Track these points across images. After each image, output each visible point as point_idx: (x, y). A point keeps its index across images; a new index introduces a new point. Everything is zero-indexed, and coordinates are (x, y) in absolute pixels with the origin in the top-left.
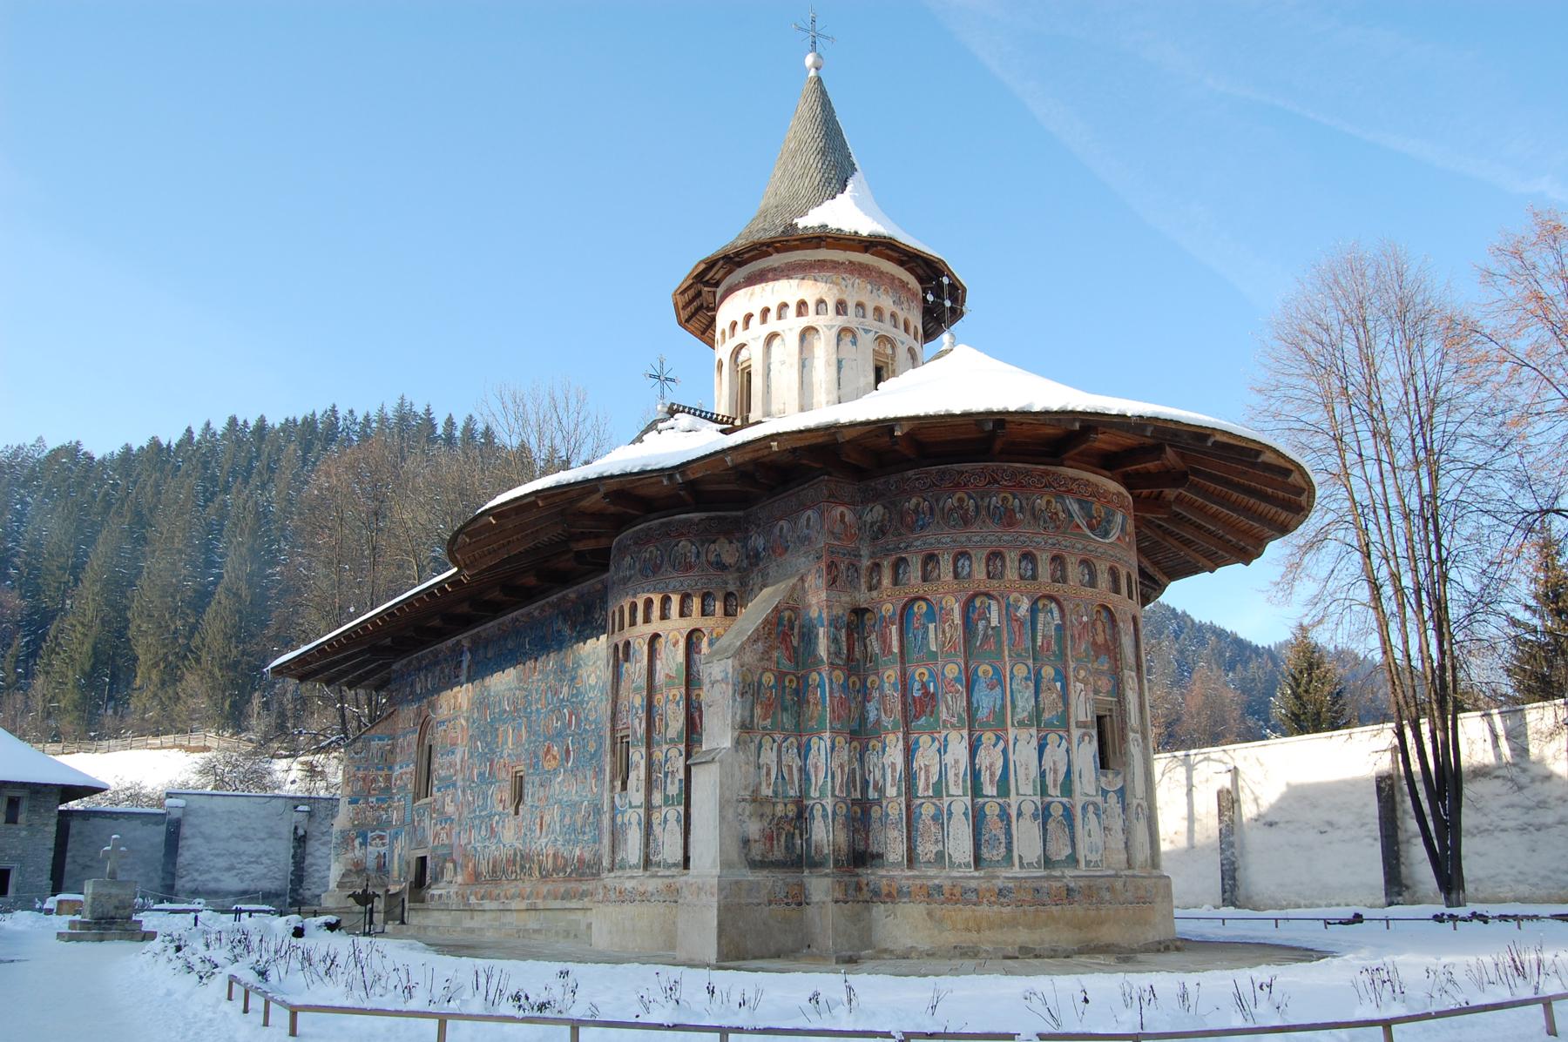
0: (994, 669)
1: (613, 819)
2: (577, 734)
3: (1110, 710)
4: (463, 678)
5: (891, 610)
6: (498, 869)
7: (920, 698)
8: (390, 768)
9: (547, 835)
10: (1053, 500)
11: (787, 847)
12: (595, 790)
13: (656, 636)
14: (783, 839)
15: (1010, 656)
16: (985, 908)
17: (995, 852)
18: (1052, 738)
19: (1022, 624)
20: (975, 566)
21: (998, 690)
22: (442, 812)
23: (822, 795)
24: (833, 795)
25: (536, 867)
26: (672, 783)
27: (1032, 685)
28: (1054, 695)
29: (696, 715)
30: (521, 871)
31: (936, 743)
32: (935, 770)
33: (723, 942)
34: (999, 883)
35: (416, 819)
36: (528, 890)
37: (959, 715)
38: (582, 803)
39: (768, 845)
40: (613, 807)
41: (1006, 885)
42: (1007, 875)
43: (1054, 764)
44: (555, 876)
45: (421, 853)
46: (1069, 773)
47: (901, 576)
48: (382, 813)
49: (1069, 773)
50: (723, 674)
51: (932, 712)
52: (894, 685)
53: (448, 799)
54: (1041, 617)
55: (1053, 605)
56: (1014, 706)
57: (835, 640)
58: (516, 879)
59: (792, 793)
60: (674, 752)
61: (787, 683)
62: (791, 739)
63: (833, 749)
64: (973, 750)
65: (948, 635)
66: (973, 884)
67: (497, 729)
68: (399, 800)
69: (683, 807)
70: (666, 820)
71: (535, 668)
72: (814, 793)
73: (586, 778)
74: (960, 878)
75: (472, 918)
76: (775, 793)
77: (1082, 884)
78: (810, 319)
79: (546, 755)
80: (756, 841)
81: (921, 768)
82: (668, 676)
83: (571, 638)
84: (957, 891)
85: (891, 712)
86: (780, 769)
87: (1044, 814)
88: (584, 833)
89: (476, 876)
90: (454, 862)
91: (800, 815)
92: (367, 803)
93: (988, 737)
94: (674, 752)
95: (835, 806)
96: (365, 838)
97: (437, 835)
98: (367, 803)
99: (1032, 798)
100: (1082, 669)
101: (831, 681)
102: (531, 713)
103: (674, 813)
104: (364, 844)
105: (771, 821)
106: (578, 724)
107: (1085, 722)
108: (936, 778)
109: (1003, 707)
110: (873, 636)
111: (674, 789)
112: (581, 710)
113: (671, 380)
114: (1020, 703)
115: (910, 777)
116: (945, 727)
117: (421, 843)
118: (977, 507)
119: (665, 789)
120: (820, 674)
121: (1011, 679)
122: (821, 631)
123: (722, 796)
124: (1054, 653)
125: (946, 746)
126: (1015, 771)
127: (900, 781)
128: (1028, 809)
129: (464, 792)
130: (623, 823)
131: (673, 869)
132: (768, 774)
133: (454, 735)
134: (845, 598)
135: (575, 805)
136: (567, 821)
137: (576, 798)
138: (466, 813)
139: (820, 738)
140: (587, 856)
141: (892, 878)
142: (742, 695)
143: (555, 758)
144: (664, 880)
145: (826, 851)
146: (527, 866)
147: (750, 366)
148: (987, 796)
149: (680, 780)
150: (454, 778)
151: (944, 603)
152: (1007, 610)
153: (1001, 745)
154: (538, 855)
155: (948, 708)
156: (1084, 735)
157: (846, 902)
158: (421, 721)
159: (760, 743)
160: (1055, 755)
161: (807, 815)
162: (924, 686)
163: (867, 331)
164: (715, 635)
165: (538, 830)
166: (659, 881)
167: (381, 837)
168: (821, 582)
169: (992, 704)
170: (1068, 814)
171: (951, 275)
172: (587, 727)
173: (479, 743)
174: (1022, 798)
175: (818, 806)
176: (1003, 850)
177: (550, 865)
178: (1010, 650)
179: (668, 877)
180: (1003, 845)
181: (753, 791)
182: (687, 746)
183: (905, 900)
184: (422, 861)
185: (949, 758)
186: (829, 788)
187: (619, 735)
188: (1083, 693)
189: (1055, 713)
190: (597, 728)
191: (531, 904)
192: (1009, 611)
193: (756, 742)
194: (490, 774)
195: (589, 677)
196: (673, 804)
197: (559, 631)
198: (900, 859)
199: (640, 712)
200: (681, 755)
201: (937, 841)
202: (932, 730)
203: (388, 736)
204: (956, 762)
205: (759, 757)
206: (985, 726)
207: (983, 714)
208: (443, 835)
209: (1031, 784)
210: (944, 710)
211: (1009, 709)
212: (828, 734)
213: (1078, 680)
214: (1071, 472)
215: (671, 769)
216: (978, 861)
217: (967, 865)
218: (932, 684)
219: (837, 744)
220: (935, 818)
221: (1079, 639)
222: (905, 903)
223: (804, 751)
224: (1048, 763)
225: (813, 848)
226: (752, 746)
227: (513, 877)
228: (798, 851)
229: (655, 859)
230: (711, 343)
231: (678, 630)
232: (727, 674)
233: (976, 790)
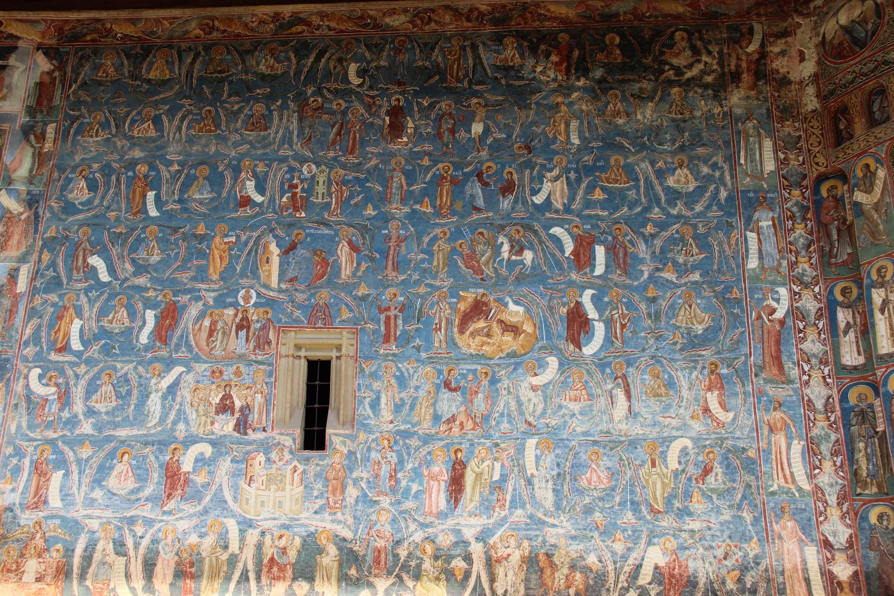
9: (487, 507)
12: (726, 417)
71: (396, 129)
73: (671, 384)
79: (466, 320)
83: (566, 90)
102: (385, 219)
135: (633, 444)
165: (439, 498)
173: (96, 261)
195: (661, 175)
197: (506, 69)
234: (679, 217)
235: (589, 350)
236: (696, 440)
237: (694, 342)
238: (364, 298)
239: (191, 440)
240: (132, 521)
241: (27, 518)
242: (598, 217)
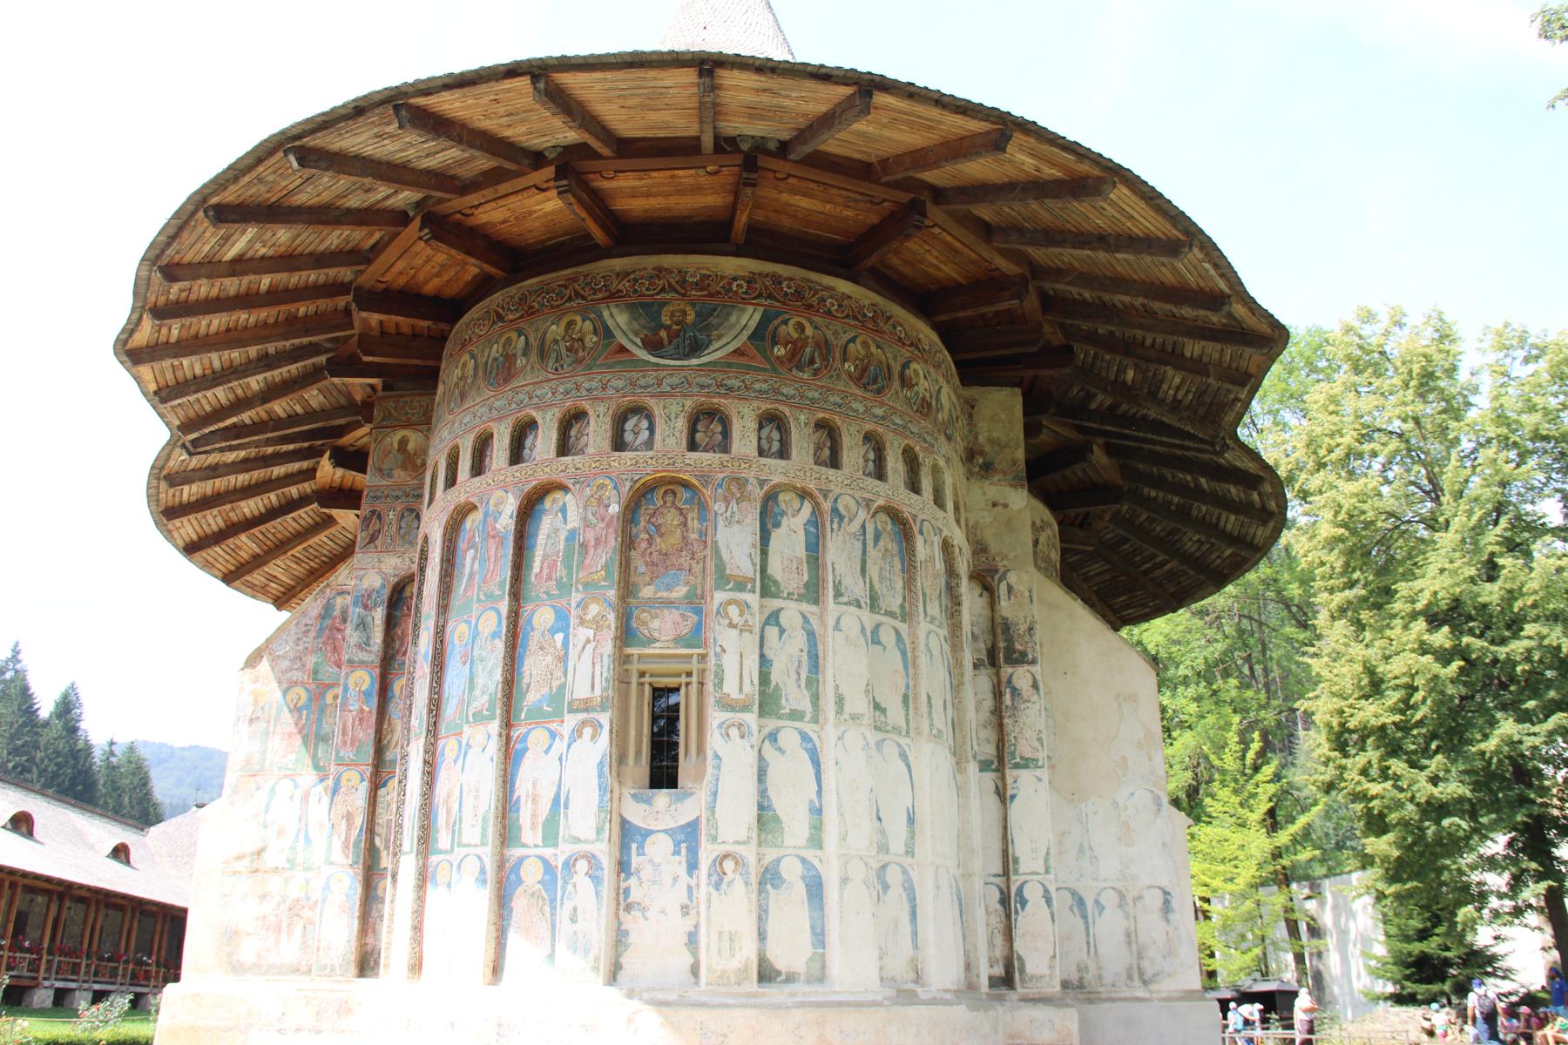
3: (689, 674)
10: (578, 319)
11: (304, 945)
14: (301, 925)
18: (538, 737)
28: (549, 658)
46: (556, 800)
76: (292, 863)
99: (480, 851)
100: (595, 600)
105: (279, 905)
107: (586, 701)
114: (480, 681)
118: (476, 368)
124: (559, 582)
156: (584, 723)
157: (318, 1032)
159: (273, 789)
174: (465, 851)
178: (480, 587)
188: (590, 647)
189: (547, 689)
205: (267, 810)
207: (450, 710)
213: (582, 622)
214: (618, 264)
219: (343, 782)
224: (522, 787)
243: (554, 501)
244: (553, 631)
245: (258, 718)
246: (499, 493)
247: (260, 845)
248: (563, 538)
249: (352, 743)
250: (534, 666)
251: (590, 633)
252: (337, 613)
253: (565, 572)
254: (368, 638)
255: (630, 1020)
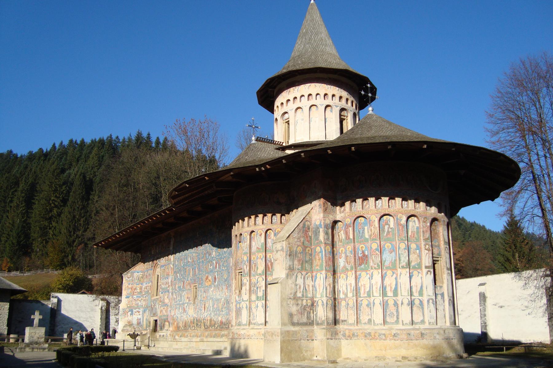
0: (392, 245)
1: (236, 306)
2: (220, 271)
4: (171, 248)
5: (350, 221)
6: (187, 325)
7: (362, 257)
8: (142, 284)
13: (253, 232)
14: (306, 312)
15: (398, 240)
16: (388, 341)
17: (392, 319)
19: (403, 227)
20: (384, 203)
21: (393, 254)
22: (164, 302)
23: (322, 297)
24: (326, 296)
25: (203, 325)
26: (260, 291)
27: (407, 251)
28: (416, 256)
29: (269, 264)
30: (197, 326)
31: (368, 276)
32: (368, 286)
33: (282, 355)
34: (394, 332)
35: (153, 305)
36: (200, 334)
37: (378, 264)
38: (222, 299)
39: (300, 316)
40: (236, 301)
41: (397, 332)
42: (397, 328)
43: (416, 283)
44: (210, 328)
45: (155, 318)
46: (422, 287)
47: (353, 208)
48: (139, 302)
49: (422, 287)
50: (281, 248)
51: (366, 263)
52: (351, 252)
53: (166, 297)
54: (411, 224)
55: (416, 219)
56: (400, 260)
57: (327, 233)
58: (194, 329)
59: (309, 296)
60: (260, 279)
61: (307, 251)
62: (309, 274)
63: (326, 278)
64: (383, 278)
65: (373, 231)
66: (383, 332)
67: (186, 269)
68: (146, 297)
69: (264, 301)
70: (257, 307)
72: (318, 296)
73: (223, 289)
74: (378, 329)
75: (177, 344)
76: (303, 295)
77: (427, 332)
78: (313, 101)
79: (206, 280)
80: (295, 315)
81: (362, 286)
82: (258, 248)
84: (377, 335)
85: (350, 262)
86: (305, 286)
87: (412, 304)
88: (223, 311)
89: (178, 328)
90: (169, 322)
91: (313, 305)
92: (133, 298)
93: (389, 273)
94: (260, 279)
95: (327, 301)
96: (132, 311)
97: (161, 311)
98: (133, 298)
101: (325, 251)
102: (200, 262)
103: (261, 303)
104: (132, 314)
105: (301, 307)
106: (219, 267)
108: (367, 290)
109: (395, 260)
110: (342, 232)
111: (261, 294)
112: (221, 262)
113: (257, 127)
114: (402, 259)
115: (357, 290)
116: (372, 269)
117: (155, 315)
119: (257, 294)
120: (320, 247)
121: (399, 250)
122: (321, 230)
123: (281, 296)
124: (416, 238)
125: (372, 277)
126: (400, 286)
127: (353, 290)
128: (406, 301)
129: (172, 294)
130: (240, 307)
131: (261, 326)
132: (300, 288)
133: (167, 271)
134: (331, 216)
136: (215, 306)
137: (219, 297)
138: (173, 302)
139: (321, 274)
140: (224, 320)
141: (350, 330)
142: (290, 255)
143: (210, 281)
144: (257, 330)
145: (323, 319)
146: (199, 324)
147: (289, 121)
148: (389, 297)
149: (263, 290)
150: (168, 288)
151: (371, 218)
152: (397, 221)
153: (395, 276)
154: (203, 320)
155: (373, 261)
156: (429, 271)
157: (332, 339)
158: (154, 265)
159: (297, 275)
160: (416, 280)
161: (315, 304)
162: (363, 252)
163: (337, 106)
164: (277, 231)
165: (203, 310)
166: (255, 330)
167: (139, 312)
168: (321, 210)
169: (391, 259)
170: (421, 302)
171: (371, 84)
172: (223, 268)
173: (178, 275)
174: (403, 297)
175: (320, 301)
176: (395, 318)
177: (208, 324)
178: (398, 237)
179: (258, 329)
180: (395, 316)
181: (294, 295)
182: (266, 276)
183: (356, 338)
184: (156, 321)
185: (373, 282)
186: (325, 294)
187: (238, 271)
188: (428, 254)
190: (227, 269)
191: (201, 339)
192: (398, 223)
193: (295, 275)
194: (183, 287)
196: (260, 300)
198: (354, 322)
199: (246, 262)
200: (263, 280)
201: (368, 315)
202: (366, 270)
203: (140, 271)
204: (377, 283)
205: (296, 281)
206: (388, 268)
207: (387, 263)
208: (164, 311)
209: (407, 292)
210: (372, 262)
211: (398, 261)
212: (324, 272)
213: (426, 249)
215: (259, 286)
216: (385, 322)
217: (381, 324)
218: (366, 251)
219: (328, 276)
220: (367, 305)
221: (426, 232)
222: (355, 339)
223: (314, 279)
225: (318, 318)
226: (294, 277)
227: (193, 328)
228: (312, 319)
229: (253, 322)
230: (272, 111)
231: (262, 229)
232: (283, 247)
233: (384, 294)
234: (225, 256)
235: (216, 283)
236: (224, 298)
237: (226, 280)
238: (198, 277)
239: (186, 303)
240: (181, 316)
241: (175, 316)
242: (217, 258)
243: (412, 219)
244: (416, 249)
245: (291, 255)
246: (400, 215)
247: (296, 290)
248: (415, 228)
249: (328, 266)
250: (413, 257)
251: (427, 251)
252: (306, 226)
253: (417, 236)
254: (329, 237)
255: (444, 332)
